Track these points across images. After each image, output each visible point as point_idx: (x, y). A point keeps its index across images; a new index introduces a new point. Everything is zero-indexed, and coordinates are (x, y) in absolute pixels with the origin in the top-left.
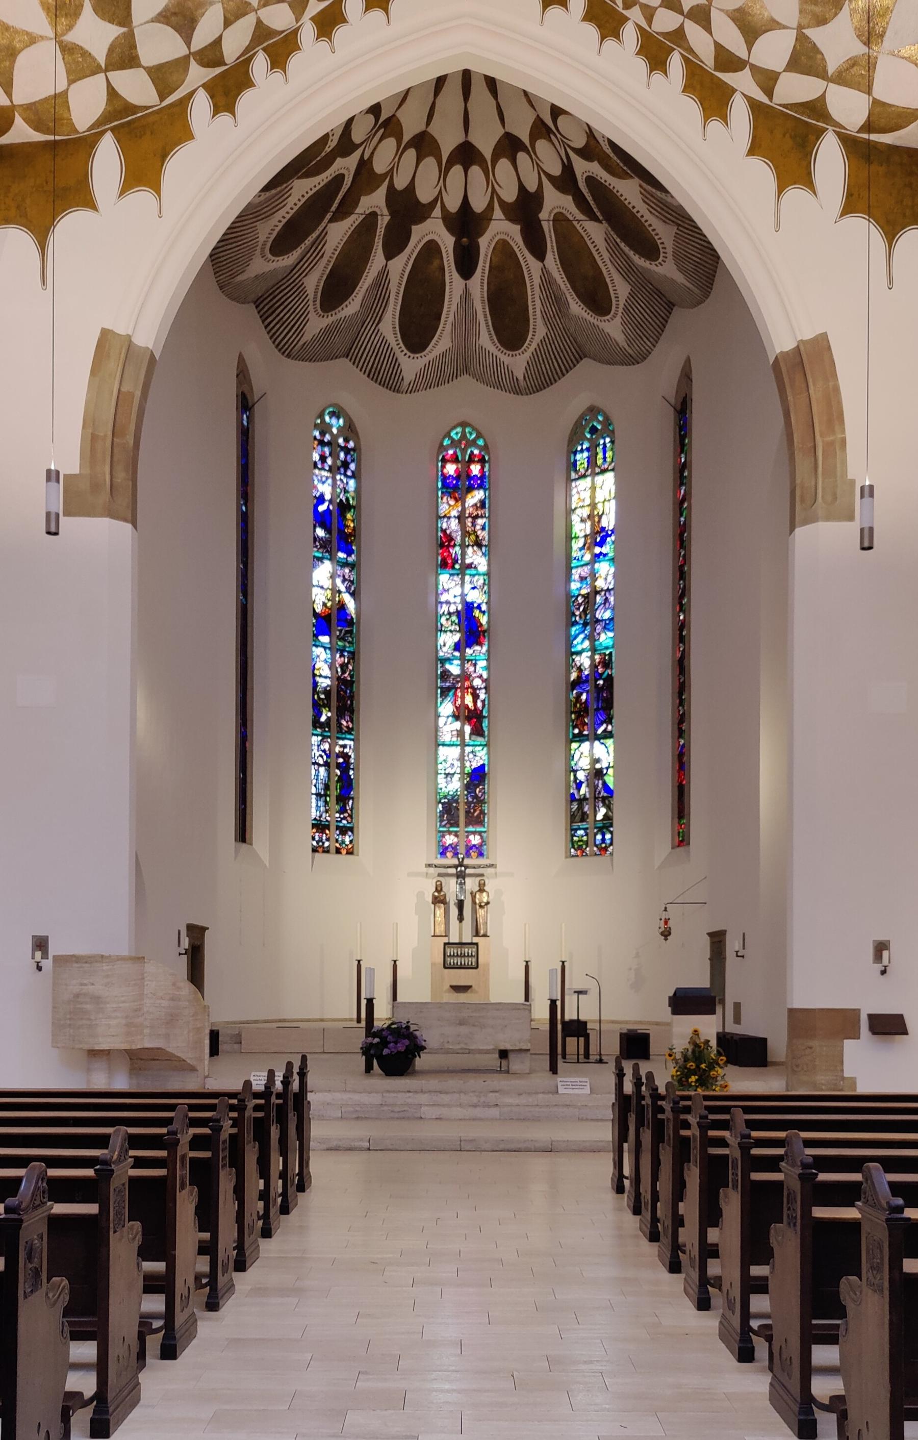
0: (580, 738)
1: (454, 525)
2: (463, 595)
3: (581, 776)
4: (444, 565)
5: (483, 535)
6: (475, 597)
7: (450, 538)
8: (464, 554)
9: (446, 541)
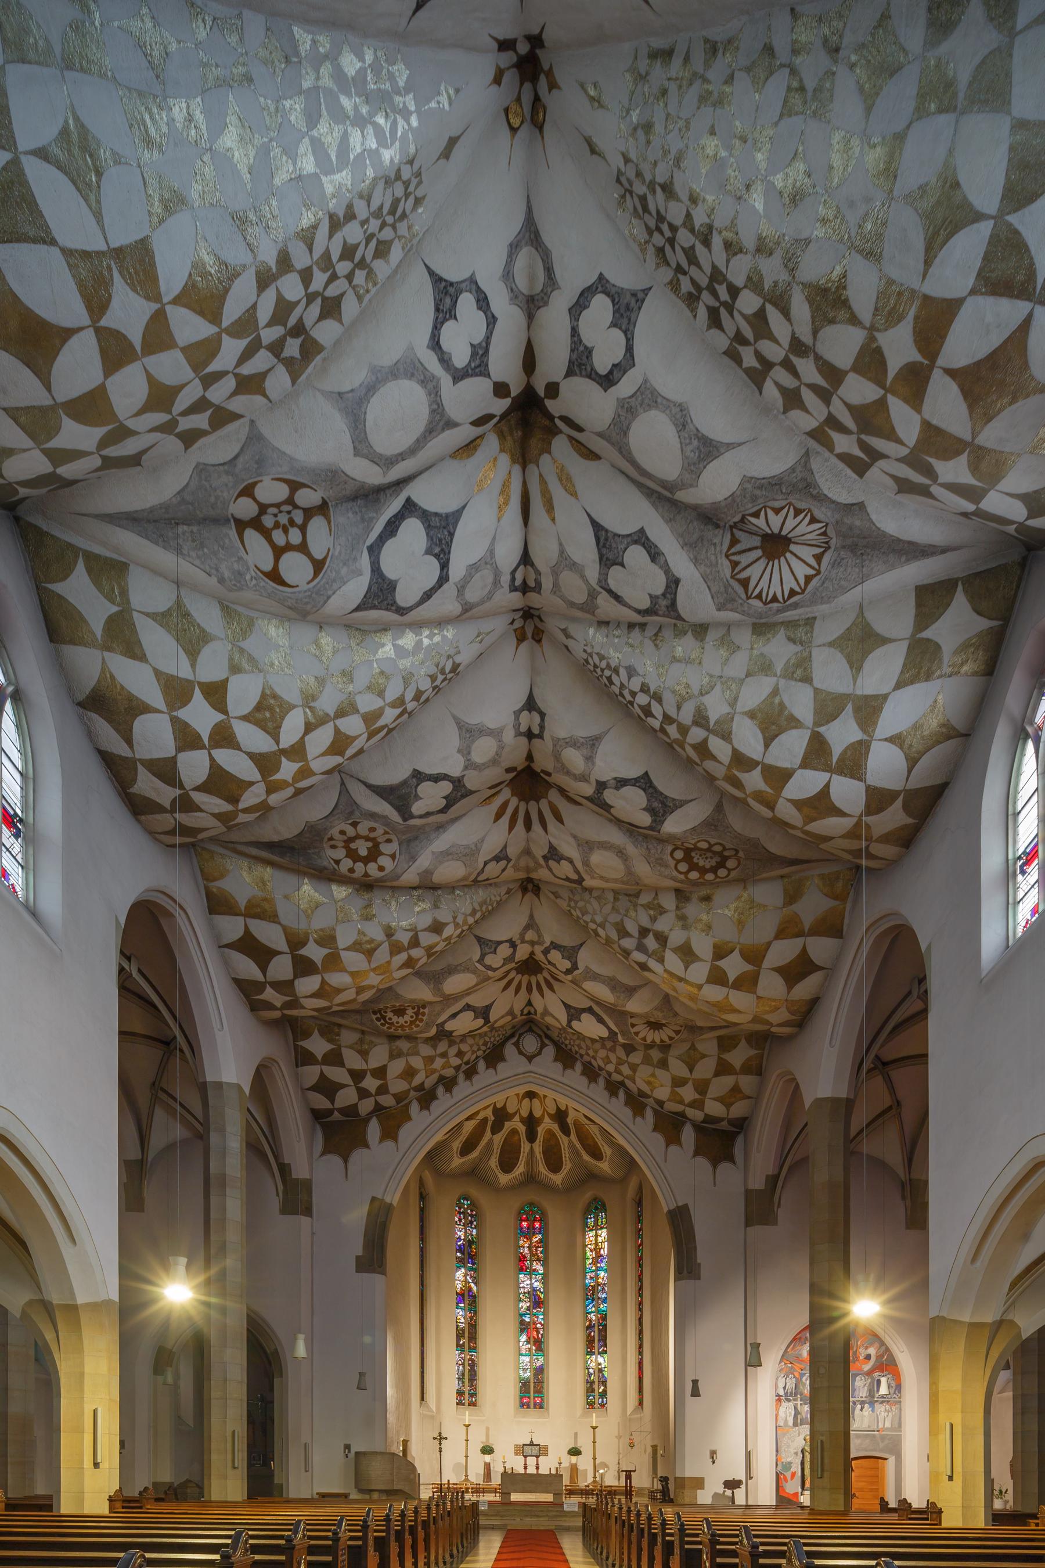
0: (591, 1353)
1: (526, 1251)
2: (531, 1284)
3: (591, 1371)
4: (522, 1269)
5: (541, 1255)
6: (536, 1284)
7: (524, 1257)
8: (531, 1265)
9: (522, 1259)
